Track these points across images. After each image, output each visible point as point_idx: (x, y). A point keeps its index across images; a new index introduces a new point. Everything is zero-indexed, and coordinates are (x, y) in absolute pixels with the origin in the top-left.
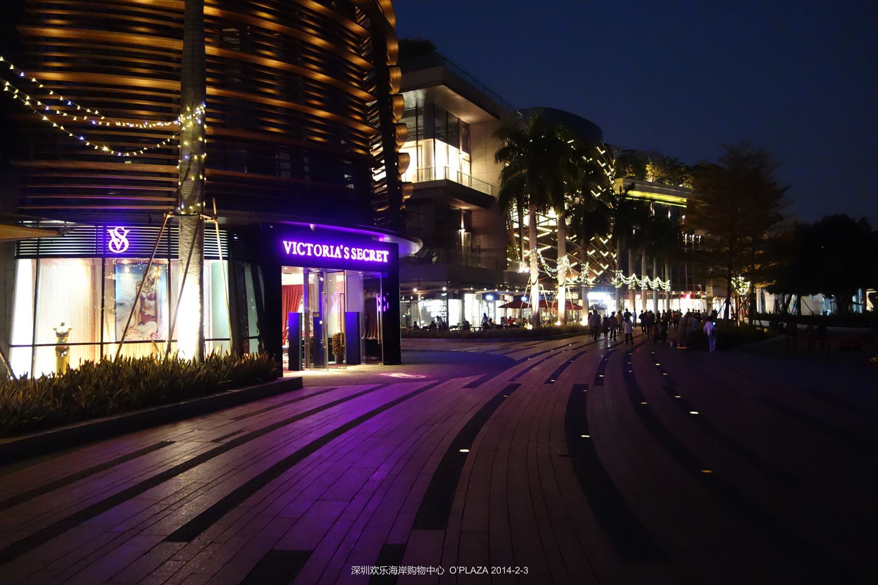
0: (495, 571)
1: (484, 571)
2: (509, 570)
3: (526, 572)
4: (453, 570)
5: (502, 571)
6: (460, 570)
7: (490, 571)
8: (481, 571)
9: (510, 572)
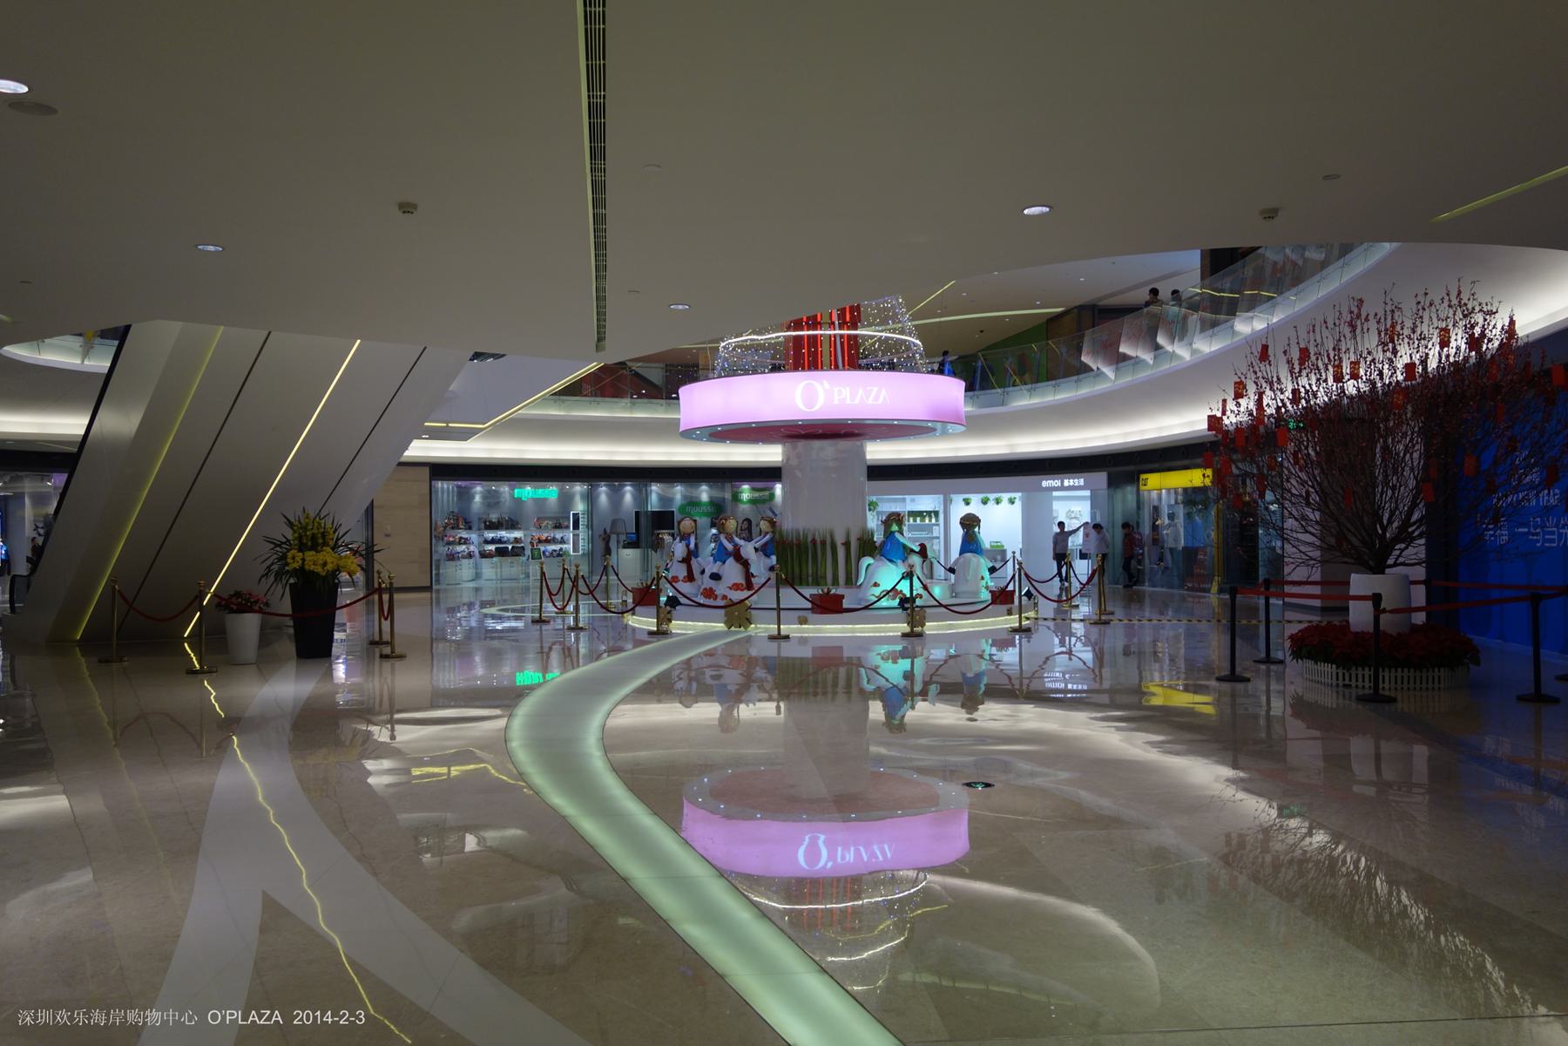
0: (301, 1020)
1: (274, 1019)
2: (328, 1018)
3: (360, 1020)
4: (214, 1017)
5: (315, 1018)
6: (228, 1018)
7: (288, 1018)
8: (269, 1018)
9: (330, 1020)
